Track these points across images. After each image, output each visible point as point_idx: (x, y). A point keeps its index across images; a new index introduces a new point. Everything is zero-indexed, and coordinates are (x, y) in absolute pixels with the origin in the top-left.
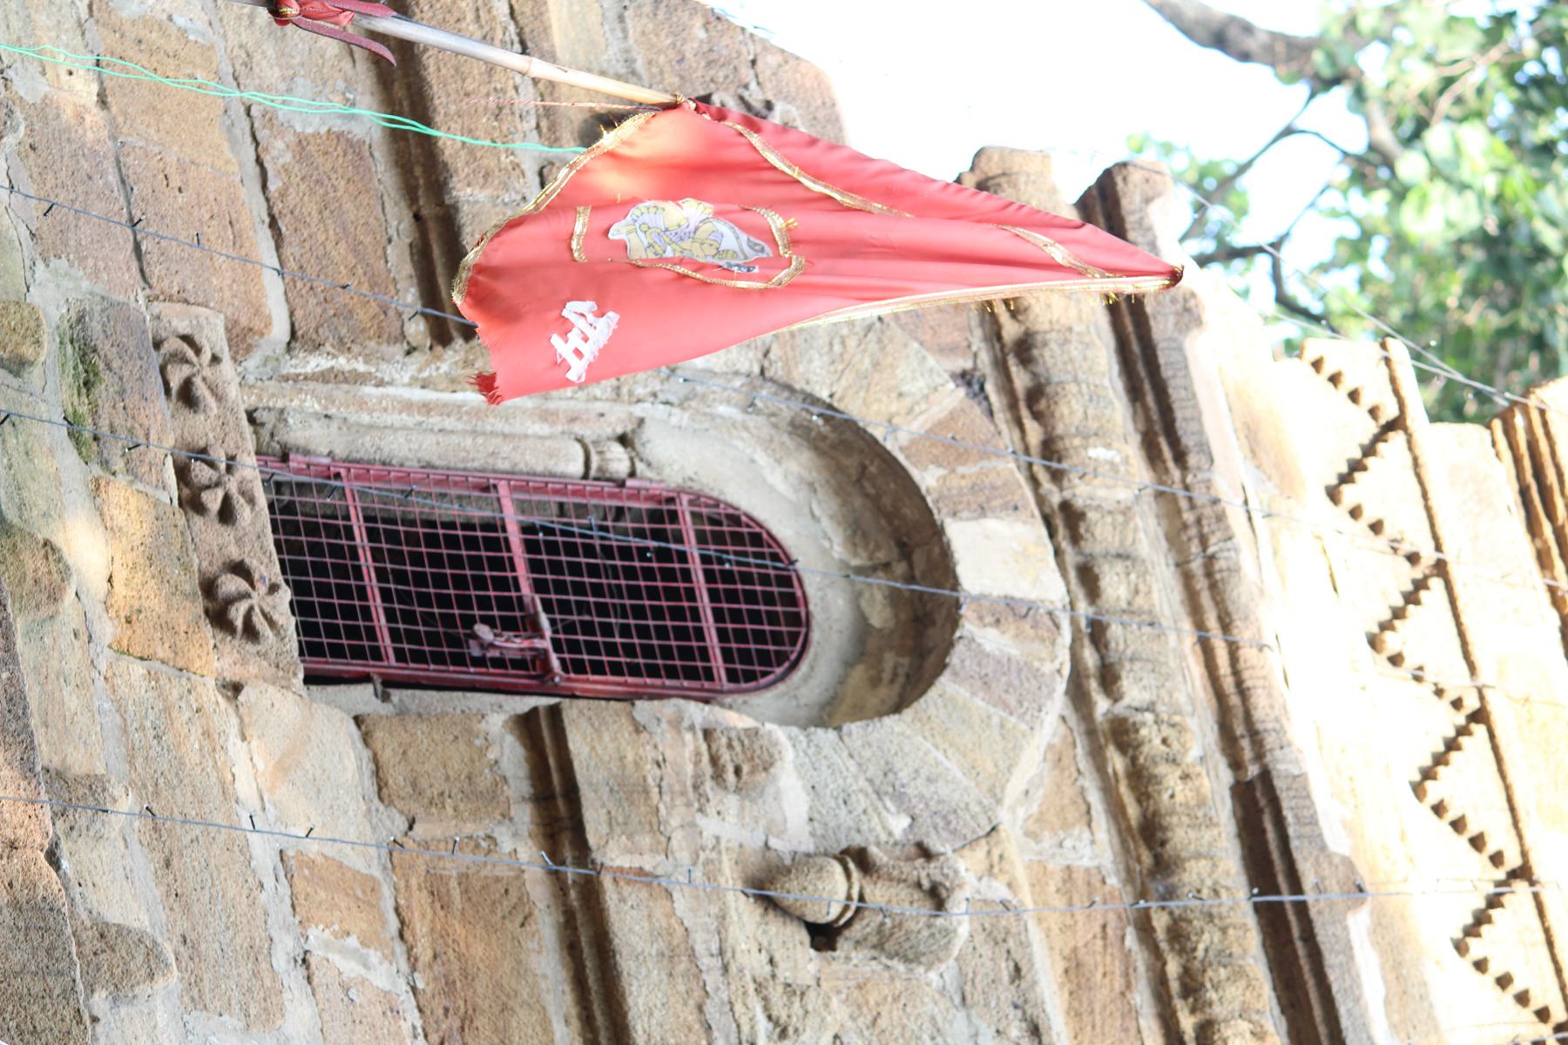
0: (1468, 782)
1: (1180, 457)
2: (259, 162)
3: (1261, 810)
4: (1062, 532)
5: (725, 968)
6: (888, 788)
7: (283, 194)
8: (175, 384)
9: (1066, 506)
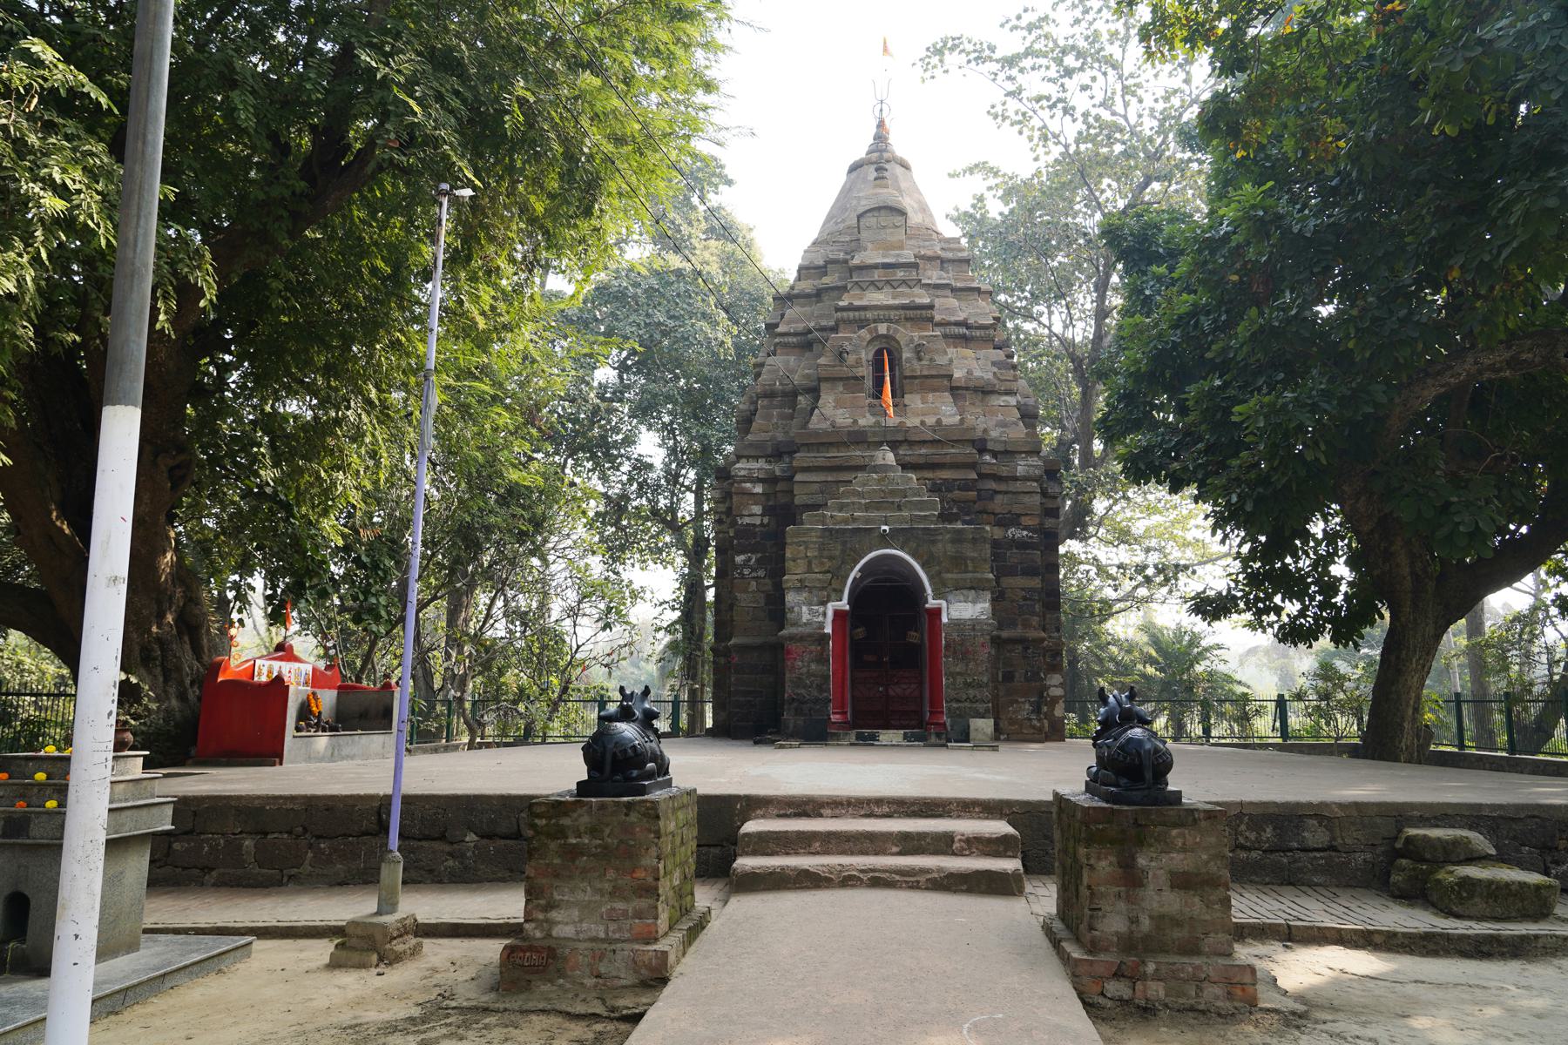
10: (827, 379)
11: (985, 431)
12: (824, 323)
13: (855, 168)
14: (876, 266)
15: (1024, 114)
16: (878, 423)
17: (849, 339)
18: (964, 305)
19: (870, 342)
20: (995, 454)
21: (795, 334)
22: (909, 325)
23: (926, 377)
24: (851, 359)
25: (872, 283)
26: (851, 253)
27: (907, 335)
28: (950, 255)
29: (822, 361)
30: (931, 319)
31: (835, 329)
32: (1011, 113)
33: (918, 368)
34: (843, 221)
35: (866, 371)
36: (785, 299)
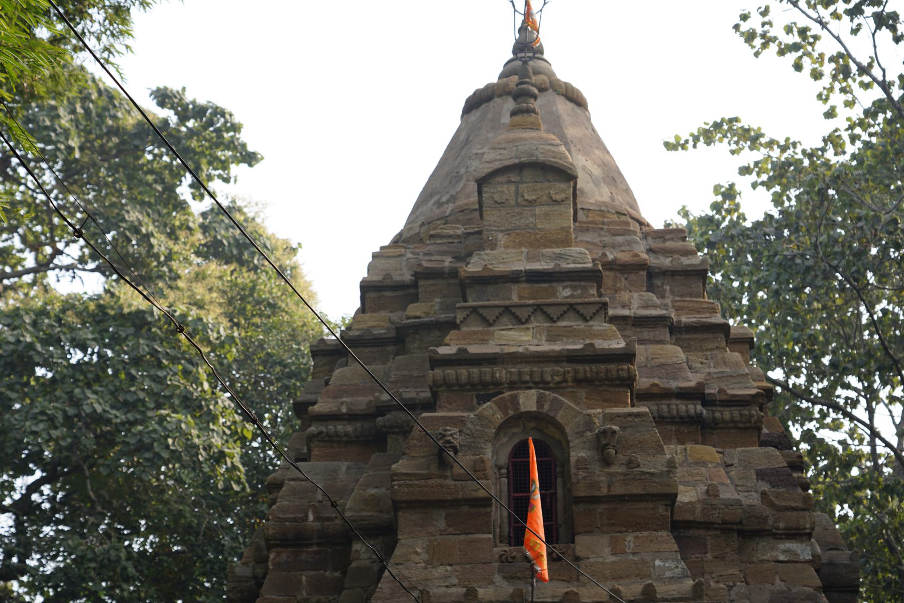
0: (553, 312)
1: (496, 358)
3: (571, 358)
6: (580, 434)
10: (412, 505)
12: (410, 393)
13: (477, 102)
14: (514, 278)
15: (803, 32)
16: (519, 594)
17: (461, 421)
18: (696, 359)
21: (351, 417)
22: (582, 393)
25: (507, 310)
26: (464, 257)
28: (666, 262)
29: (401, 466)
30: (628, 381)
31: (430, 406)
32: (777, 31)
34: (453, 199)
35: (495, 487)
36: (329, 354)
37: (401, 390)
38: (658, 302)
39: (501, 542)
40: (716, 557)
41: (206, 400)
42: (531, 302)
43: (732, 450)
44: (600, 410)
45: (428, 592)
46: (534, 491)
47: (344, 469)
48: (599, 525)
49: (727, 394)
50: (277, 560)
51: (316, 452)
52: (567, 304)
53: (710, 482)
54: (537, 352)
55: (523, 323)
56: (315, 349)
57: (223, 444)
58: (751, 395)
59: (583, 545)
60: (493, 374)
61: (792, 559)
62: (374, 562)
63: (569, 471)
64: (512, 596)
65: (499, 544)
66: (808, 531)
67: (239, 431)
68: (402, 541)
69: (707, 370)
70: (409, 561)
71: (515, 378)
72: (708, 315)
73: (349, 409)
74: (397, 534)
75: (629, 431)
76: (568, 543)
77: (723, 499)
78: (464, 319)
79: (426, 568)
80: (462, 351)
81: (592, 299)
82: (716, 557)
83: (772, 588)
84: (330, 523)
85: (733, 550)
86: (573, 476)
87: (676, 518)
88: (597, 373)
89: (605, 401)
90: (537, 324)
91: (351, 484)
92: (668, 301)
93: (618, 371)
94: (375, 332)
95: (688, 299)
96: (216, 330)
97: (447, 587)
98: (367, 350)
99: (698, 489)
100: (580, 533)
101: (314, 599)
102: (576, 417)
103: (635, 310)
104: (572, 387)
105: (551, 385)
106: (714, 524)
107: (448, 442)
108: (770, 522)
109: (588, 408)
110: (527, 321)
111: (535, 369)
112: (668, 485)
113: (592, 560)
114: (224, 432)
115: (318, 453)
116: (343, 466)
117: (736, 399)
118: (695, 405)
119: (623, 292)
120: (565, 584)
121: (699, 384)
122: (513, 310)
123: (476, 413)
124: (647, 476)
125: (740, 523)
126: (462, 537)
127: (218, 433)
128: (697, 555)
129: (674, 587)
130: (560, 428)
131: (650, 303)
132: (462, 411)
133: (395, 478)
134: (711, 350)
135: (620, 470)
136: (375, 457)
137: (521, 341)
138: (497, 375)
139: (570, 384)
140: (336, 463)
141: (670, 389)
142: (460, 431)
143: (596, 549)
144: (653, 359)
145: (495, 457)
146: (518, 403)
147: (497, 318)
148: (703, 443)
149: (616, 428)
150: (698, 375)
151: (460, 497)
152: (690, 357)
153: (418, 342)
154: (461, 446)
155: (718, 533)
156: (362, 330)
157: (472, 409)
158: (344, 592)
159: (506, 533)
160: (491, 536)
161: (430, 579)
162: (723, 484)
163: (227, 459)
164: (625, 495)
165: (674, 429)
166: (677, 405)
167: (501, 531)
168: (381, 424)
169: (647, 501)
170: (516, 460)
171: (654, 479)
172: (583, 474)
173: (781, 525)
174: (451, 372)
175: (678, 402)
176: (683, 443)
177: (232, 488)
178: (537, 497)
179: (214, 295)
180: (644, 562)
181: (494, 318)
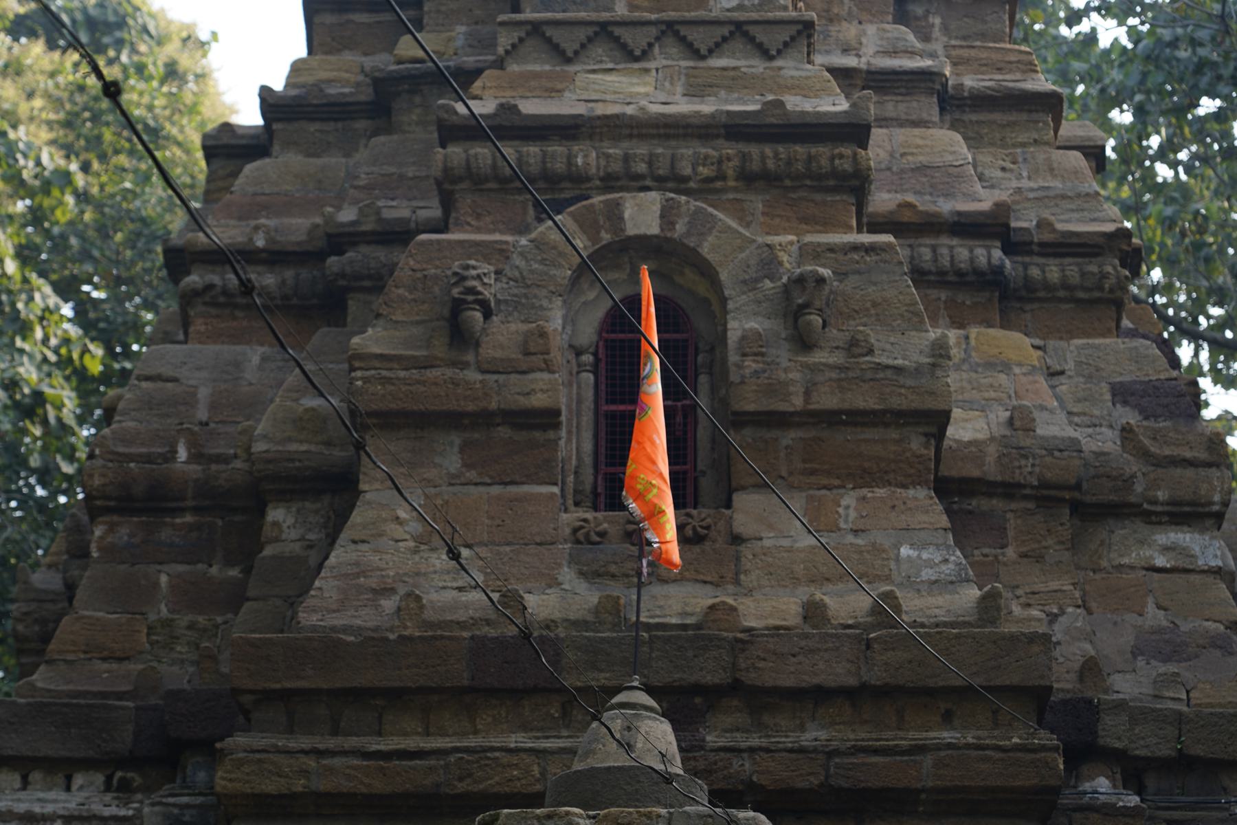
1: (577, 127)
2: (476, 484)
3: (735, 129)
4: (613, 184)
5: (847, 368)
6: (750, 284)
7: (491, 477)
8: (598, 539)
9: (601, 179)
10: (392, 421)
11: (1091, 669)
16: (610, 610)
17: (501, 253)
19: (583, 269)
20: (1133, 772)
21: (275, 257)
22: (757, 203)
23: (831, 419)
24: (501, 335)
27: (750, 244)
30: (856, 184)
33: (794, 379)
35: (565, 389)
37: (380, 203)
38: (919, 45)
39: (577, 504)
40: (1024, 556)
41: (9, 292)
42: (653, 17)
43: (1063, 344)
44: (793, 238)
45: (418, 599)
46: (647, 376)
47: (256, 360)
48: (784, 474)
49: (1054, 230)
50: (109, 539)
51: (198, 326)
52: (730, 22)
53: (1015, 403)
54: (663, 115)
55: (637, 59)
56: (209, 143)
57: (41, 380)
58: (1104, 234)
59: (749, 510)
60: (570, 158)
61: (1182, 563)
62: (310, 547)
63: (724, 360)
64: (597, 611)
65: (572, 508)
66: (1216, 508)
67: (75, 356)
68: (368, 496)
69: (1015, 184)
70: (381, 535)
71: (617, 167)
72: (1018, 76)
73: (270, 240)
74: (358, 481)
75: (853, 280)
76: (717, 508)
77: (1042, 438)
78: (514, 46)
79: (416, 551)
80: (507, 109)
81: (780, 14)
82: (1024, 556)
83: (1140, 621)
84: (222, 467)
85: (1062, 543)
86: (733, 369)
87: (944, 471)
88: (789, 163)
89: (805, 220)
90: (665, 62)
91: (264, 393)
92: (938, 47)
93: (832, 158)
94: (332, 91)
95: (978, 43)
96: (32, 155)
97: (460, 589)
98: (313, 127)
99: (992, 416)
100: (743, 488)
101: (184, 620)
102: (742, 249)
103: (869, 57)
104: (736, 189)
105: (692, 184)
106: (1020, 486)
107: (472, 291)
108: (1139, 488)
109: (768, 234)
110: (645, 55)
111: (660, 150)
112: (932, 393)
113: (767, 543)
114: (45, 360)
115: (203, 328)
116: (254, 355)
117: (1074, 240)
118: (988, 248)
119: (845, 24)
120: (709, 588)
121: (998, 205)
122: (617, 31)
123: (533, 235)
124: (889, 373)
125: (1078, 487)
126: (496, 490)
127: (31, 356)
128: (986, 551)
129: (940, 601)
130: (707, 271)
131: (900, 44)
132: (502, 233)
133: (357, 364)
134: (1023, 145)
135: (831, 361)
136: (323, 336)
137: (631, 95)
138: (580, 161)
139: (731, 183)
140: (238, 348)
141: (936, 215)
142: (498, 273)
143: (773, 521)
144: (903, 155)
145: (569, 329)
146: (621, 218)
147: (583, 46)
148: (1002, 327)
149: (826, 272)
150: (997, 192)
151: (493, 405)
152: (980, 157)
153: (418, 111)
154: (498, 302)
155: (1031, 505)
156: (304, 86)
157: (523, 230)
158: (247, 605)
159: (588, 487)
160: (556, 490)
161: (425, 574)
162: (1043, 408)
163: (49, 407)
164: (838, 413)
165: (943, 296)
166: (951, 248)
167: (577, 481)
168: (335, 269)
169: (886, 425)
170: (613, 336)
171: (902, 381)
172: (754, 365)
173: (1161, 495)
174: (482, 153)
175: (955, 242)
176: (961, 326)
177: (58, 468)
178: (655, 389)
179: (38, 103)
180: (876, 549)
181: (577, 46)
